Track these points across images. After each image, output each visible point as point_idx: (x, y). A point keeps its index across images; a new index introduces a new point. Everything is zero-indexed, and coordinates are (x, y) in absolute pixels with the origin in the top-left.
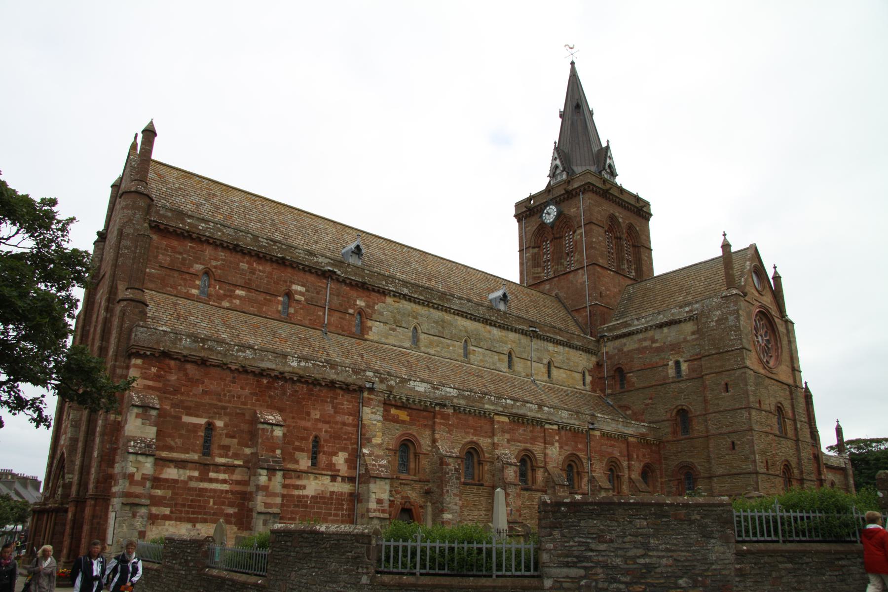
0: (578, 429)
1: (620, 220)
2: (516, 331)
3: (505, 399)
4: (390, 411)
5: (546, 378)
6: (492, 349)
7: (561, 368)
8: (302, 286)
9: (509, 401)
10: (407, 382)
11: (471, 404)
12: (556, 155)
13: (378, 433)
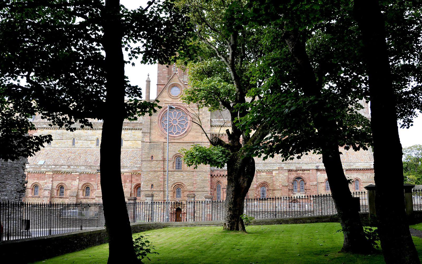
6: (87, 139)
9: (53, 167)
11: (35, 170)
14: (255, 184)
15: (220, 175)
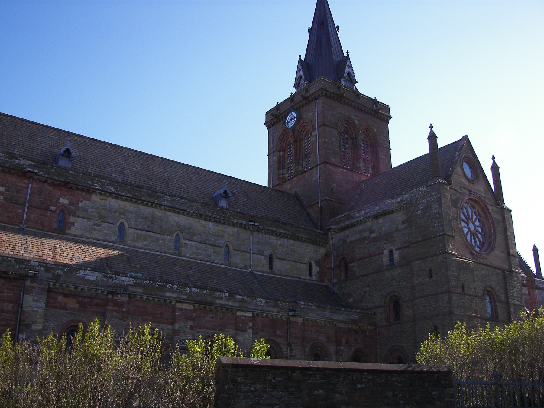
0: (276, 316)
1: (357, 122)
2: (234, 225)
3: (190, 288)
4: (58, 298)
5: (267, 268)
7: (284, 260)
10: (77, 271)
12: (300, 67)
13: (39, 320)
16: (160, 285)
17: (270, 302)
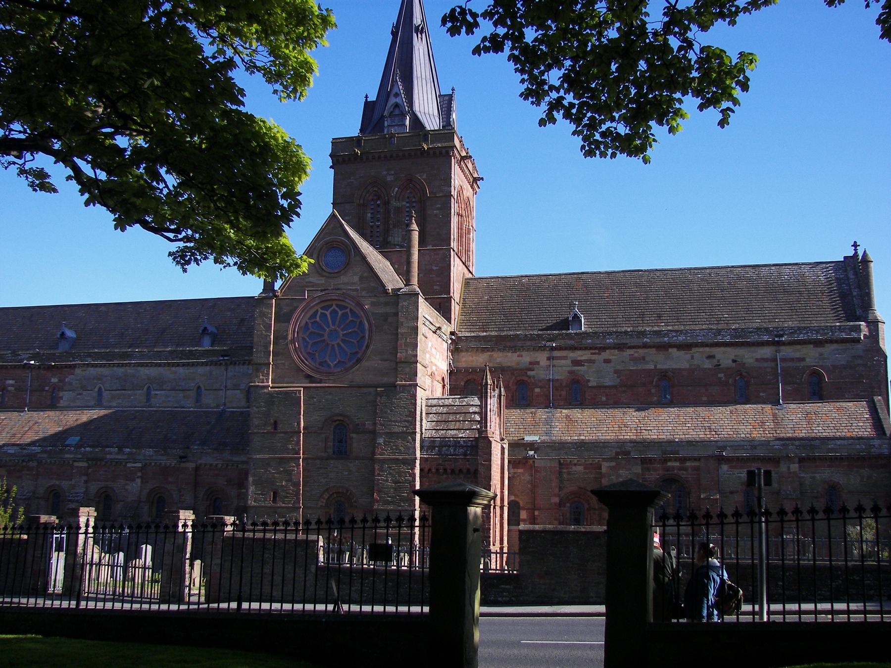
8: (13, 380)
14: (555, 495)
15: (445, 470)
16: (61, 449)
17: (159, 451)
